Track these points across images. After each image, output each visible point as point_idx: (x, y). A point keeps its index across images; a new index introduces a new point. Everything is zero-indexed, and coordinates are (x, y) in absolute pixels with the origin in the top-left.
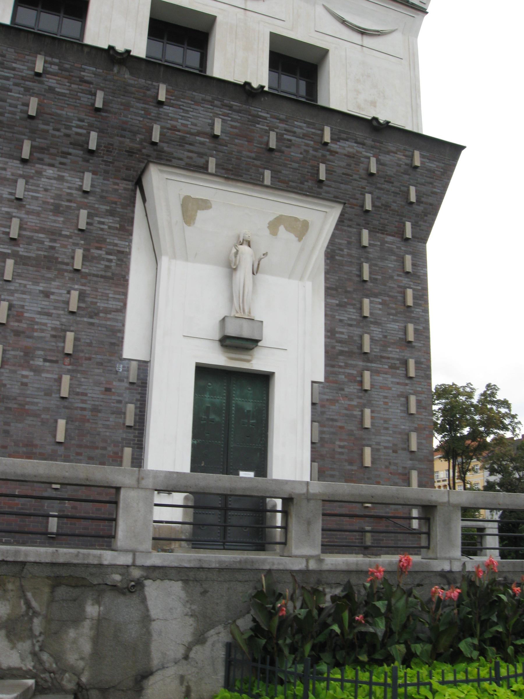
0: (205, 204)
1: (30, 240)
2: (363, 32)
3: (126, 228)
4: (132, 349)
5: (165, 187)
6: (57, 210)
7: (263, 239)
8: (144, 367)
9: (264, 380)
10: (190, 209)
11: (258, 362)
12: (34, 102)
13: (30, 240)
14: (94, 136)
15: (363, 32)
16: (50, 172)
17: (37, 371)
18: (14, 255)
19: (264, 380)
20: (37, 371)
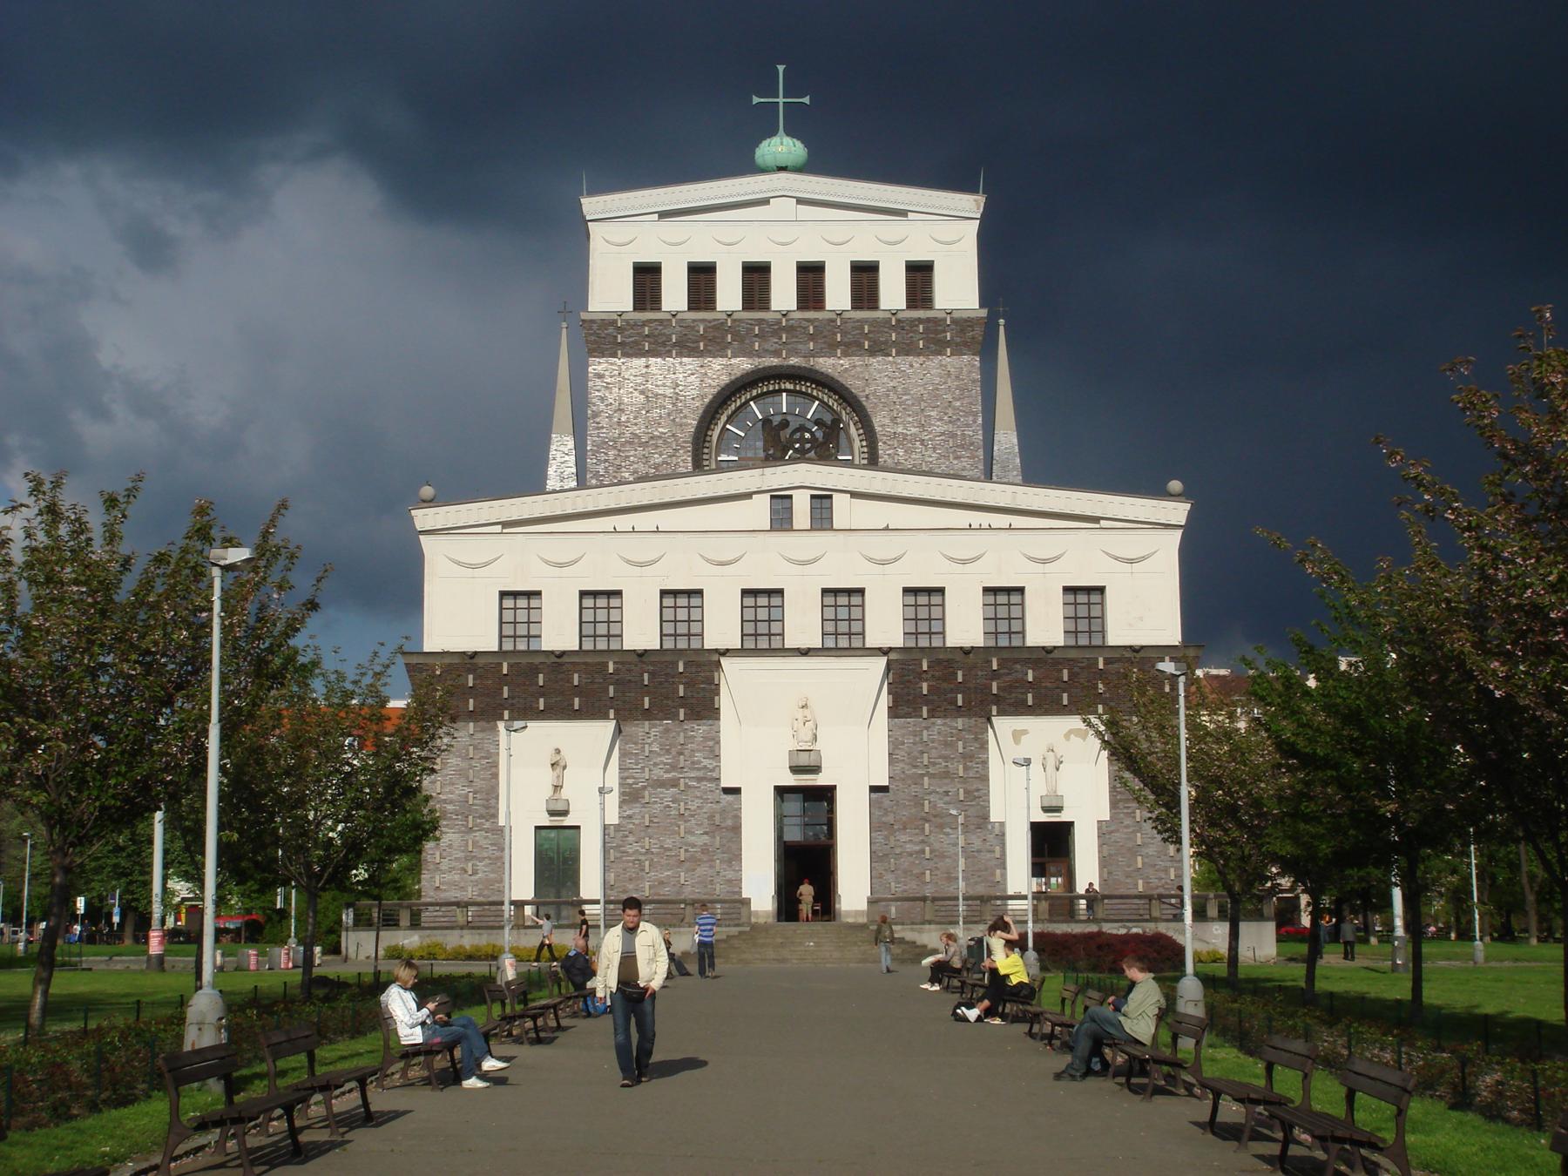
0: (1025, 732)
1: (934, 764)
2: (1131, 561)
3: (984, 746)
4: (995, 816)
5: (1004, 726)
6: (946, 744)
7: (1062, 748)
8: (1002, 824)
9: (1068, 827)
10: (1017, 736)
11: (1063, 817)
12: (925, 686)
13: (934, 764)
14: (960, 696)
15: (1131, 561)
16: (939, 721)
17: (947, 834)
18: (928, 774)
19: (1068, 827)
20: (947, 834)
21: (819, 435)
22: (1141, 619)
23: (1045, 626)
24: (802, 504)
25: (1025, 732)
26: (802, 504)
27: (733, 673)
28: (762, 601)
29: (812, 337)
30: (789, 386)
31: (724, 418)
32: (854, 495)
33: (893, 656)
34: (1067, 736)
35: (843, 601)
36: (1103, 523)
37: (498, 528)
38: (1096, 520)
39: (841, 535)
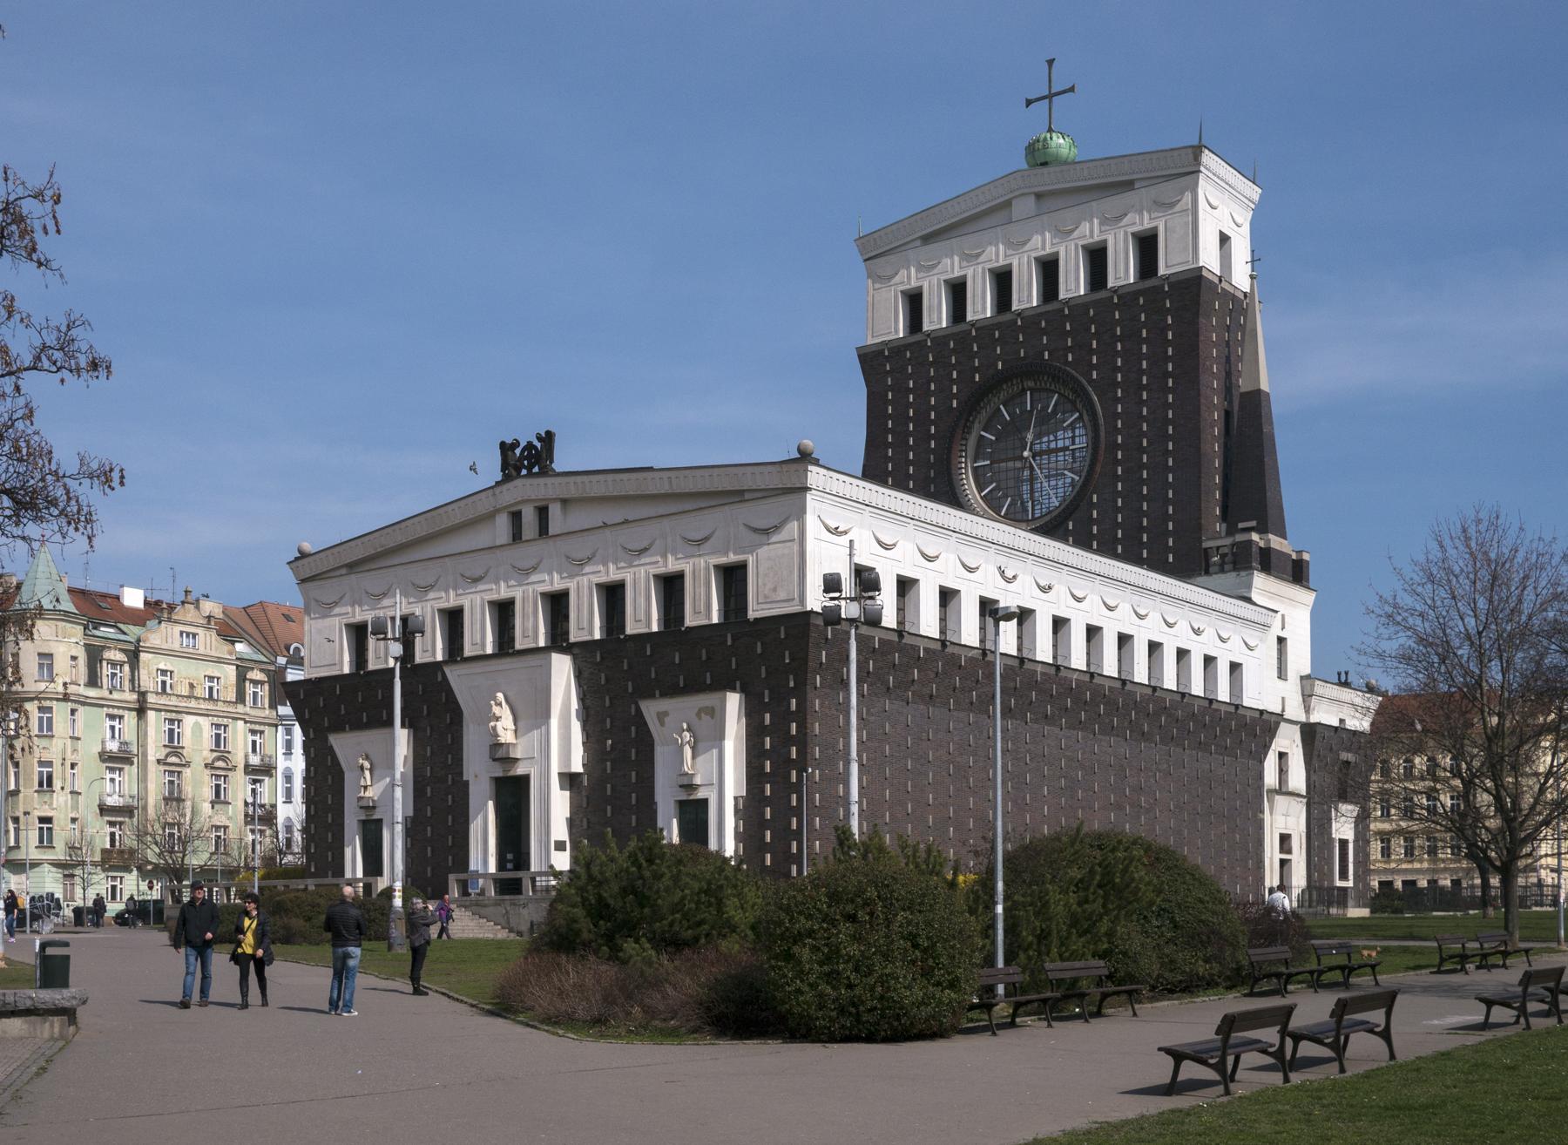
0: (666, 714)
10: (661, 717)
21: (539, 445)
22: (775, 590)
23: (705, 607)
24: (529, 516)
25: (666, 714)
26: (529, 516)
27: (454, 675)
28: (504, 612)
29: (1044, 332)
30: (1031, 384)
31: (976, 425)
32: (565, 502)
33: (576, 651)
34: (698, 715)
35: (557, 604)
36: (747, 496)
37: (344, 571)
38: (741, 492)
39: (551, 542)
